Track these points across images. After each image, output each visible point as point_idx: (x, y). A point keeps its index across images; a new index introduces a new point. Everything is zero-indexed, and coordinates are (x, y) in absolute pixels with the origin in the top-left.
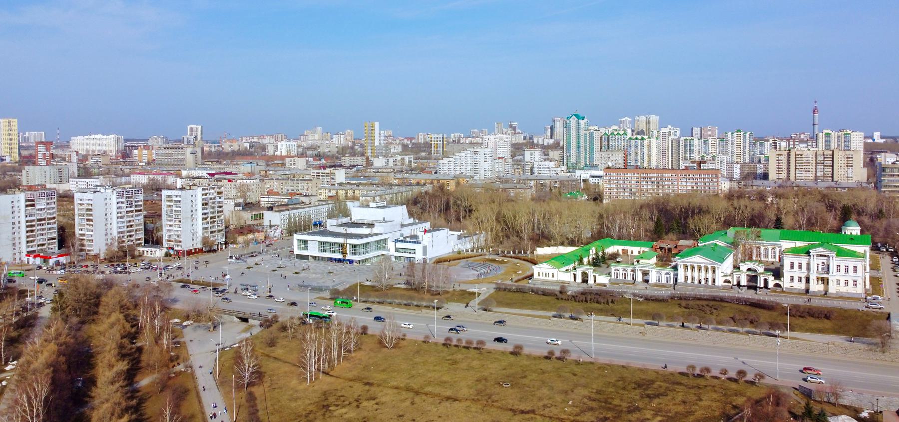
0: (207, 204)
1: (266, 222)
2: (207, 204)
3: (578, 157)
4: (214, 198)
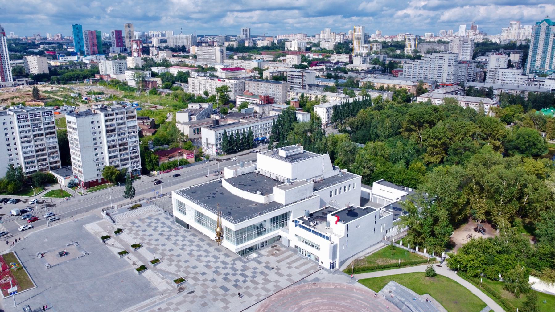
0: (113, 131)
1: (204, 140)
2: (113, 131)
3: (543, 63)
4: (124, 124)
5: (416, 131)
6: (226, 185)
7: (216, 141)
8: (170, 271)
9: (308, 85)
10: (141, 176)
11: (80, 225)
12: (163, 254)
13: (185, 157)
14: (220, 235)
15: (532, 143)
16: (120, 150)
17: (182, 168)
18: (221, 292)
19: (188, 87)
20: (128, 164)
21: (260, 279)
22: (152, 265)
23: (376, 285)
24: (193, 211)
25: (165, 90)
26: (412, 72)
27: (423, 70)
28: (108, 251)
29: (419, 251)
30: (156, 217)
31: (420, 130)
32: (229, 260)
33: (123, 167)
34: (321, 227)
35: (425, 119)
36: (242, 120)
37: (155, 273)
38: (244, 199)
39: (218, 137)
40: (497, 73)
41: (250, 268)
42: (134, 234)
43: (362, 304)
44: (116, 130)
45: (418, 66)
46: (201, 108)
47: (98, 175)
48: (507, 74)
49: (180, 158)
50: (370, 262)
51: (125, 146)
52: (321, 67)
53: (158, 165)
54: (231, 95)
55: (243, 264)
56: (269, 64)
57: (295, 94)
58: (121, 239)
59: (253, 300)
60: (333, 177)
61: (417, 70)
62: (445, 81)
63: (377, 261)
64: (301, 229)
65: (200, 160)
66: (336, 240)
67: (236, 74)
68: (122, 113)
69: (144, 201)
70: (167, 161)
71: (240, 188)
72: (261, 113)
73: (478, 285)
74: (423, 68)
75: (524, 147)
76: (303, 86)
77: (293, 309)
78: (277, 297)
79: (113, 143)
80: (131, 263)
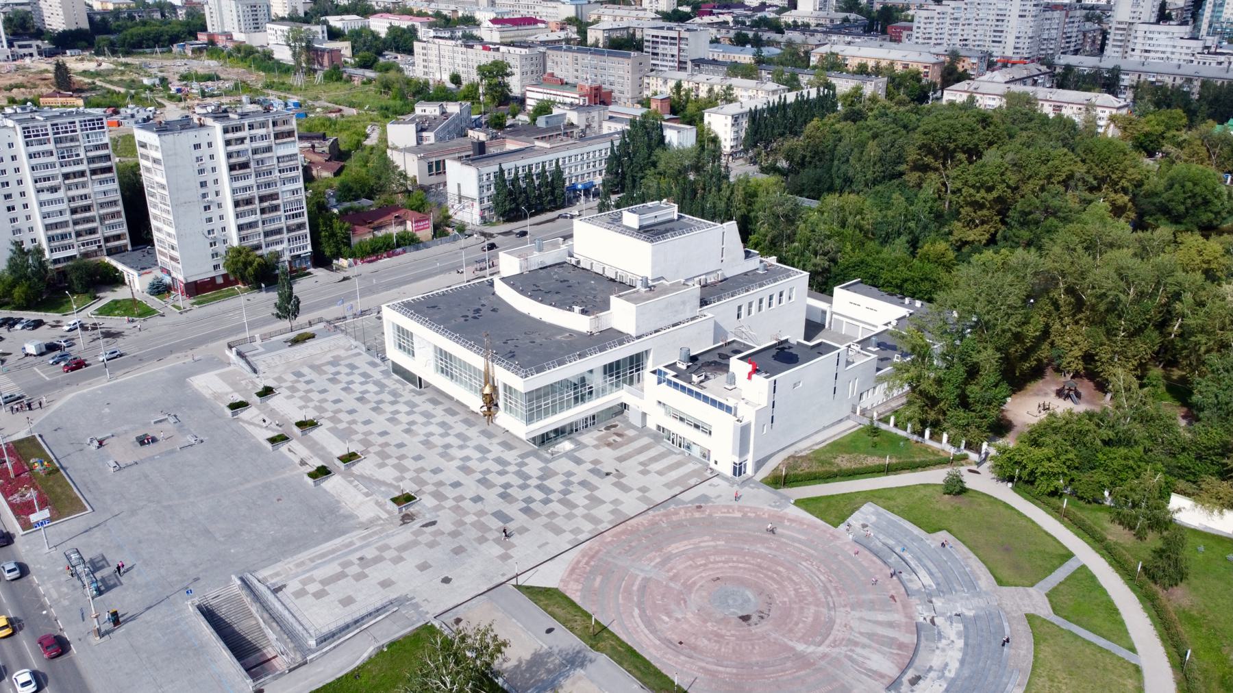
0: (245, 165)
1: (451, 189)
2: (245, 165)
4: (269, 149)
5: (936, 170)
6: (503, 291)
7: (481, 192)
8: (381, 478)
9: (692, 61)
10: (311, 270)
11: (180, 379)
12: (366, 443)
13: (409, 226)
14: (491, 402)
15: (1199, 200)
16: (263, 211)
17: (404, 252)
18: (497, 524)
19: (413, 64)
20: (282, 242)
21: (579, 496)
22: (342, 465)
23: (835, 511)
24: (431, 349)
25: (360, 71)
26: (933, 31)
27: (961, 27)
28: (245, 436)
29: (931, 438)
30: (347, 362)
31: (946, 168)
32: (511, 456)
33: (271, 249)
34: (715, 385)
35: (960, 143)
36: (538, 144)
37: (351, 482)
38: (544, 323)
39: (485, 183)
40: (1133, 33)
41: (556, 474)
42: (301, 398)
43: (803, 551)
44: (252, 164)
45: (948, 16)
46: (443, 113)
47: (216, 267)
48: (1155, 36)
49: (400, 229)
50: (823, 463)
51: (274, 202)
52: (722, 18)
53: (349, 245)
54: (515, 85)
55: (542, 465)
56: (601, 10)
57: (660, 82)
58: (272, 410)
59: (564, 541)
60: (746, 274)
61: (947, 26)
62: (1009, 53)
63: (838, 460)
64: (672, 390)
65: (445, 234)
66: (748, 414)
67: (524, 33)
68: (263, 125)
69: (321, 325)
70: (368, 237)
71: (535, 299)
72: (583, 127)
73: (1057, 513)
74: (962, 21)
75: (1182, 208)
76: (680, 62)
77: (651, 560)
78: (614, 536)
79: (246, 195)
80: (297, 461)
